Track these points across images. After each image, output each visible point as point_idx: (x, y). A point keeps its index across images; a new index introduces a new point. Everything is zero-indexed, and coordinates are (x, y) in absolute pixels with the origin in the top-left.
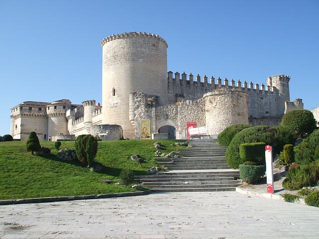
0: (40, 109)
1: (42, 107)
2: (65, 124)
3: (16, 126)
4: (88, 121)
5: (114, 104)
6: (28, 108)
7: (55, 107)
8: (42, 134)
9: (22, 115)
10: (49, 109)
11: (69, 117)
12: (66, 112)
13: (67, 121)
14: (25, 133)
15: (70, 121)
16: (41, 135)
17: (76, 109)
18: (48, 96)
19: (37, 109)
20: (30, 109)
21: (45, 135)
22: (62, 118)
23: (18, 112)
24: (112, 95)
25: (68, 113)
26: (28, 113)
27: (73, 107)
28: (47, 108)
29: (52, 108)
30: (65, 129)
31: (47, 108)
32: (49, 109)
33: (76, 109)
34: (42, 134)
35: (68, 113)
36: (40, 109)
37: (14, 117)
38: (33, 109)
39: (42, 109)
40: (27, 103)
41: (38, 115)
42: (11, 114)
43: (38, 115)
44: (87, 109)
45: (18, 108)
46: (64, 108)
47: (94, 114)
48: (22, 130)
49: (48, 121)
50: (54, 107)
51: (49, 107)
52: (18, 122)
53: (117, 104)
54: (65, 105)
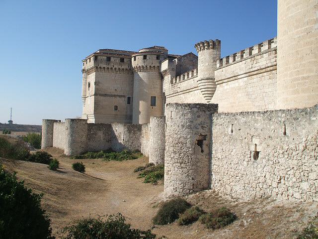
0: (122, 60)
1: (124, 57)
2: (158, 82)
3: (89, 84)
4: (207, 76)
6: (106, 58)
7: (145, 57)
8: (124, 96)
9: (97, 68)
11: (165, 71)
12: (160, 63)
13: (162, 78)
14: (101, 95)
15: (167, 78)
17: (176, 60)
18: (133, 40)
19: (118, 60)
20: (109, 59)
21: (129, 98)
22: (155, 74)
23: (91, 64)
25: (165, 65)
27: (171, 58)
28: (133, 59)
29: (140, 58)
30: (158, 90)
31: (133, 59)
32: (135, 60)
33: (176, 60)
34: (124, 96)
35: (165, 65)
36: (122, 60)
37: (87, 72)
38: (112, 59)
40: (104, 52)
41: (119, 69)
42: (83, 67)
43: (119, 69)
44: (204, 57)
45: (92, 59)
46: (158, 58)
47: (218, 65)
48: (96, 90)
49: (133, 76)
50: (142, 57)
51: (135, 57)
52: (92, 78)
54: (159, 54)
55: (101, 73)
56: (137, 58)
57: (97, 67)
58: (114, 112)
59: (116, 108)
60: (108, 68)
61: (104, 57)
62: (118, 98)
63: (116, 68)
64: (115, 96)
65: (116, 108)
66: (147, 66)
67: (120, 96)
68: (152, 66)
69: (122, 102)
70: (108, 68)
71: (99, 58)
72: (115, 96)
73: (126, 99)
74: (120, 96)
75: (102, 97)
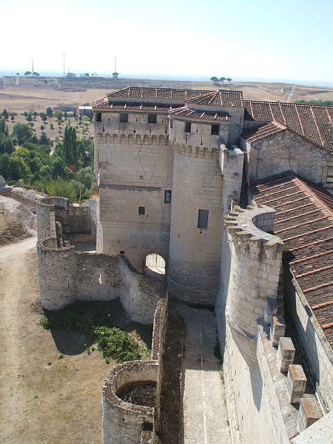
6: (117, 115)
8: (158, 189)
16: (155, 193)
19: (144, 120)
26: (116, 132)
34: (158, 189)
38: (131, 118)
41: (146, 136)
43: (146, 136)
50: (183, 124)
55: (112, 145)
58: (138, 218)
59: (142, 210)
60: (123, 136)
61: (114, 114)
62: (145, 192)
63: (138, 136)
64: (140, 188)
65: (142, 210)
67: (150, 189)
68: (202, 147)
69: (153, 201)
70: (123, 136)
72: (140, 188)
74: (150, 189)
75: (112, 193)
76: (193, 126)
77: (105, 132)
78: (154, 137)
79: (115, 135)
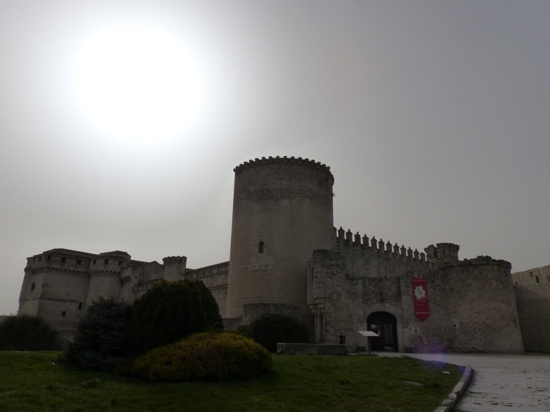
3: (33, 286)
5: (261, 266)
6: (60, 259)
8: (75, 301)
10: (95, 263)
19: (74, 262)
20: (64, 260)
21: (81, 304)
24: (257, 251)
26: (58, 267)
28: (92, 262)
31: (92, 262)
32: (95, 263)
34: (75, 301)
36: (79, 262)
38: (68, 261)
39: (82, 263)
41: (74, 271)
50: (104, 261)
53: (266, 266)
56: (97, 262)
57: (48, 267)
59: (64, 314)
60: (61, 269)
63: (70, 270)
64: (65, 301)
65: (64, 314)
66: (107, 271)
67: (71, 301)
68: (113, 271)
71: (53, 258)
72: (65, 301)
73: (78, 304)
74: (71, 301)
76: (110, 262)
77: (52, 266)
78: (78, 271)
79: (57, 269)
